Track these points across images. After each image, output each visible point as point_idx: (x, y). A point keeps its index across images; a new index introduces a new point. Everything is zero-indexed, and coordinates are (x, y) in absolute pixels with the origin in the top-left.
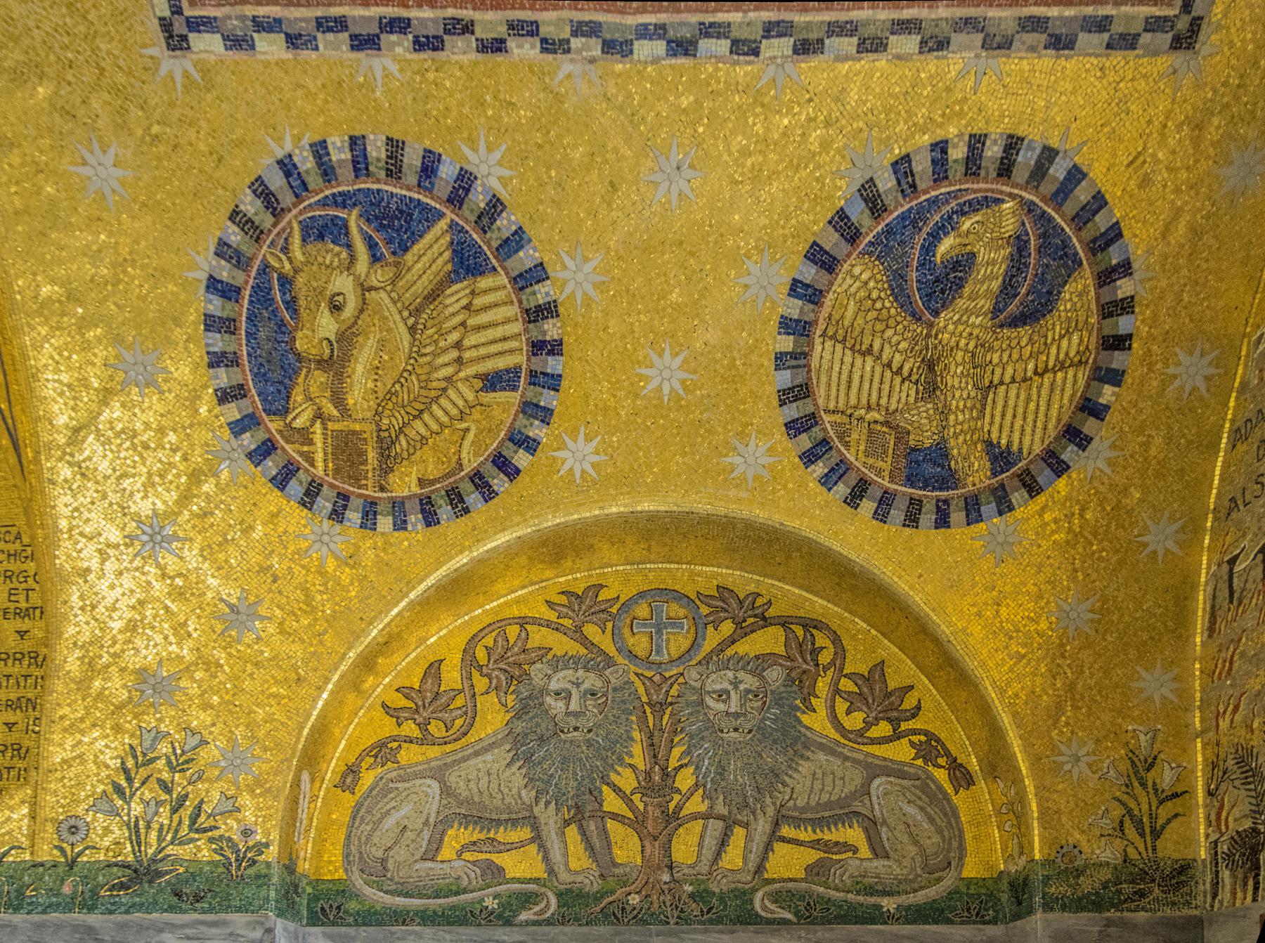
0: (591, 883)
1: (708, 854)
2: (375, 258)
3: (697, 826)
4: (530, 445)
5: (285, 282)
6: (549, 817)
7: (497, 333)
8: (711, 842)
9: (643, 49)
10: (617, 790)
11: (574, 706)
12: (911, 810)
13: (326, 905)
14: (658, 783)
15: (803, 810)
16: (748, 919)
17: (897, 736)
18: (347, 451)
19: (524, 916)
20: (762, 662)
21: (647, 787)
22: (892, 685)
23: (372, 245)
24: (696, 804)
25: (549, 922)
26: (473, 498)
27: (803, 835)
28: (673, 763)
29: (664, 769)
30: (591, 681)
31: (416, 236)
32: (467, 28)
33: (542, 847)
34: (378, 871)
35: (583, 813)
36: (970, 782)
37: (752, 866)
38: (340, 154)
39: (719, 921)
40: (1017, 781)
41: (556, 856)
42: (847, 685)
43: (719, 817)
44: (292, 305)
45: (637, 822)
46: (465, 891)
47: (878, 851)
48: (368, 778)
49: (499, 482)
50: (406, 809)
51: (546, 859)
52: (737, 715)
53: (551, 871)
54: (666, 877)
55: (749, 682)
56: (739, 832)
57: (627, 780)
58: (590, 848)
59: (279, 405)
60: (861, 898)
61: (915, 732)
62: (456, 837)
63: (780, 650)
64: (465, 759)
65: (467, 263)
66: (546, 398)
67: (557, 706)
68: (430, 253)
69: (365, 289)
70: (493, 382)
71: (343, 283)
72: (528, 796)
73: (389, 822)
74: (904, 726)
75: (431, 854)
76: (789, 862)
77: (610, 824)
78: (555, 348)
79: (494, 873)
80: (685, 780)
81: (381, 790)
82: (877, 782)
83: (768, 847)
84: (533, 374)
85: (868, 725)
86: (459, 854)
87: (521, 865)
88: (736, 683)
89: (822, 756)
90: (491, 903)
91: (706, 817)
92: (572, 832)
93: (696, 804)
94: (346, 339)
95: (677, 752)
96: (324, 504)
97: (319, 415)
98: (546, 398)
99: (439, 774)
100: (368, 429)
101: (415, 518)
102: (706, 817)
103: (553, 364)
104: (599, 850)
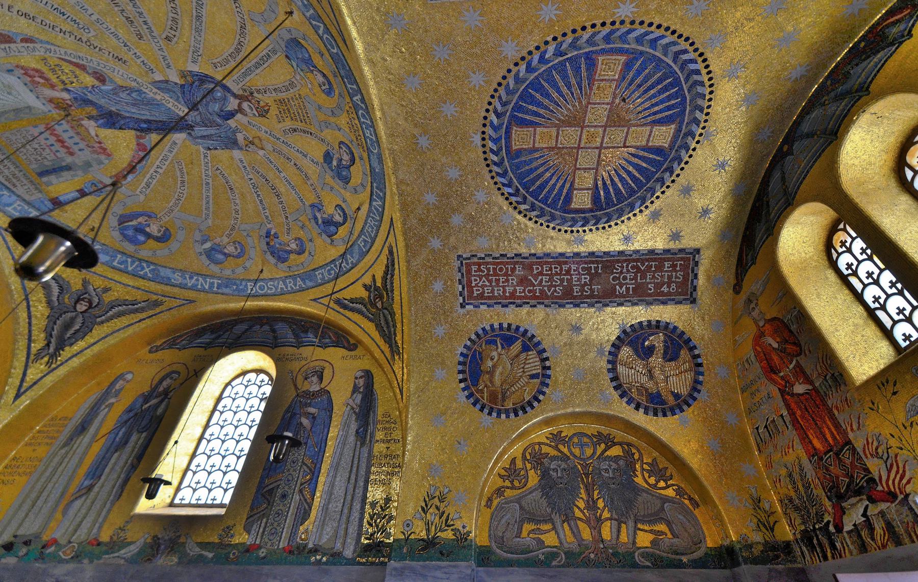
0: (575, 547)
1: (615, 536)
2: (503, 348)
3: (608, 523)
4: (544, 393)
5: (480, 353)
6: (557, 520)
7: (533, 363)
8: (614, 530)
9: (567, 306)
10: (579, 508)
11: (559, 475)
12: (680, 517)
13: (484, 558)
14: (591, 505)
15: (644, 516)
16: (635, 565)
17: (667, 487)
18: (493, 397)
19: (554, 563)
20: (617, 458)
21: (588, 507)
22: (661, 467)
23: (502, 345)
24: (606, 514)
25: (563, 566)
26: (528, 409)
27: (646, 528)
28: (596, 497)
29: (593, 499)
30: (564, 465)
31: (513, 343)
32: (528, 303)
33: (557, 532)
34: (501, 542)
35: (568, 518)
36: (698, 506)
37: (631, 541)
38: (496, 326)
39: (624, 566)
40: (716, 506)
41: (562, 536)
42: (645, 466)
43: (615, 520)
44: (481, 359)
45: (587, 522)
46: (532, 552)
47: (675, 536)
48: (495, 502)
49: (535, 404)
50: (509, 516)
51: (558, 537)
52: (613, 478)
53: (561, 543)
54: (602, 546)
55: (614, 466)
56: (623, 526)
57: (581, 504)
58: (573, 532)
59: (475, 383)
60: (674, 556)
61: (673, 485)
62: (527, 527)
63: (621, 454)
64: (526, 495)
65: (526, 348)
66: (547, 381)
67: (554, 474)
68: (517, 347)
69: (500, 354)
70: (533, 377)
71: (495, 354)
72: (549, 510)
73: (503, 521)
74: (669, 483)
75: (518, 535)
76: (644, 540)
77: (579, 522)
78: (549, 368)
79: (541, 542)
80: (601, 504)
81: (500, 507)
82: (666, 505)
83: (635, 533)
84: (543, 375)
85: (657, 482)
86: (528, 534)
87: (550, 539)
88: (610, 466)
89: (644, 495)
90: (542, 557)
91: (611, 519)
92: (566, 525)
93: (606, 514)
94: (494, 366)
95: (596, 493)
96: (486, 411)
97: (486, 386)
98: (547, 381)
99: (518, 500)
100: (500, 390)
101: (512, 415)
102: (611, 519)
103: (548, 372)
104: (576, 533)
